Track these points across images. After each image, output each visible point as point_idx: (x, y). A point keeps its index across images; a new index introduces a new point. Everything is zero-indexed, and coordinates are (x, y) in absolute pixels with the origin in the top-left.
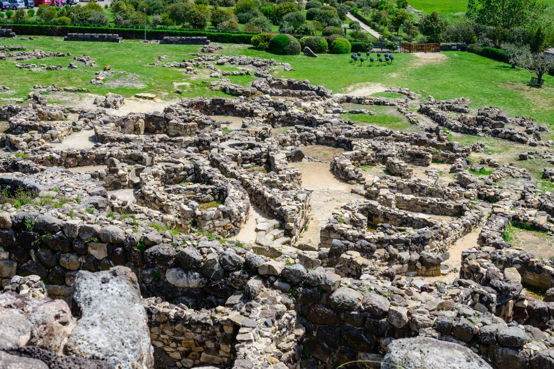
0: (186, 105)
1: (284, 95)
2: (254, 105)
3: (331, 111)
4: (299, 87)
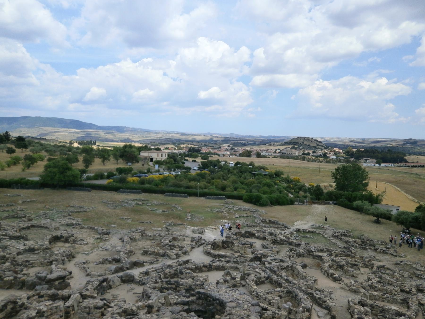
0: (234, 234)
2: (264, 234)
3: (294, 236)
4: (273, 223)
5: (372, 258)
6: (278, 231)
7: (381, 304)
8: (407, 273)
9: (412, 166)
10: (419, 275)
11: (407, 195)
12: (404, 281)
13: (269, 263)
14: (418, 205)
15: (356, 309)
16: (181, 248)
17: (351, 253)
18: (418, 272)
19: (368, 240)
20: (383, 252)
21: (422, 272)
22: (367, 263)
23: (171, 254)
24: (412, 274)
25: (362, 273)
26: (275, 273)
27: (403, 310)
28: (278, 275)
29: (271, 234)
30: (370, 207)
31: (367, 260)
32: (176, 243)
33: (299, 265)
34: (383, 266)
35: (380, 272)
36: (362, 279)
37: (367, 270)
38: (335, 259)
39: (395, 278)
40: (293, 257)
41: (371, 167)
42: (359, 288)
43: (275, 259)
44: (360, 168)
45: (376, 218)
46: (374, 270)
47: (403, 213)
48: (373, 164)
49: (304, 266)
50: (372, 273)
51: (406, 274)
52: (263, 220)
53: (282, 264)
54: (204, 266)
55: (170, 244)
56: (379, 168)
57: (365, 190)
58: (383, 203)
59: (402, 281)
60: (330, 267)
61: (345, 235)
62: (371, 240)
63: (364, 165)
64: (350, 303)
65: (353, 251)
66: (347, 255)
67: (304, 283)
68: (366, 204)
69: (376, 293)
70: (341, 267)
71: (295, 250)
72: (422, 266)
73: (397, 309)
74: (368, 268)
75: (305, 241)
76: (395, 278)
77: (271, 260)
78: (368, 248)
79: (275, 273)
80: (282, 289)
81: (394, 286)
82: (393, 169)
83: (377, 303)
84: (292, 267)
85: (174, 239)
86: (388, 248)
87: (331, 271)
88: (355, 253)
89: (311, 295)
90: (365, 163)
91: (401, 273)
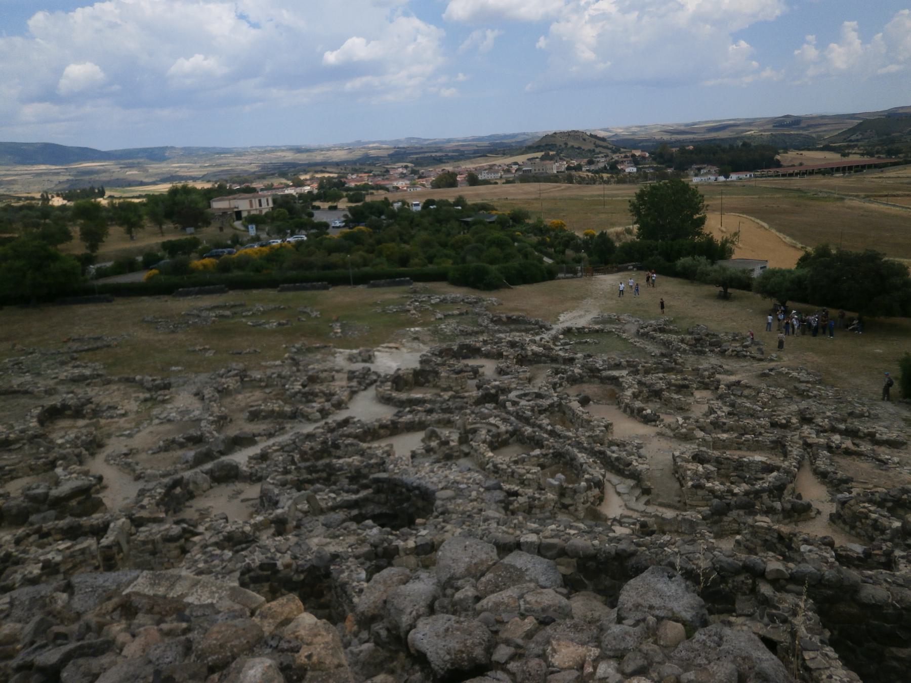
5: (715, 370)
7: (735, 455)
8: (782, 390)
9: (791, 175)
10: (804, 391)
11: (781, 236)
12: (777, 405)
13: (515, 403)
14: (801, 254)
15: (689, 470)
16: (329, 396)
17: (676, 364)
18: (803, 386)
19: (707, 335)
20: (738, 356)
21: (810, 385)
22: (707, 380)
23: (309, 410)
24: (791, 391)
25: (698, 402)
26: (527, 421)
27: (777, 461)
28: (533, 425)
29: (513, 344)
30: (709, 268)
31: (706, 373)
32: (317, 388)
33: (574, 400)
34: (739, 382)
35: (733, 394)
36: (698, 412)
37: (707, 394)
39: (760, 403)
40: (561, 385)
41: (710, 184)
42: (693, 429)
43: (525, 395)
44: (686, 188)
45: (721, 289)
46: (720, 392)
47: (774, 273)
48: (713, 178)
50: (717, 399)
51: (780, 393)
52: (495, 319)
53: (540, 402)
54: (382, 426)
55: (303, 390)
56: (725, 184)
57: (699, 234)
58: (734, 257)
59: (773, 407)
60: (635, 396)
61: (662, 330)
62: (714, 335)
63: (696, 180)
64: (678, 460)
65: (680, 360)
66: (667, 370)
67: (587, 434)
68: (702, 263)
69: (725, 436)
70: (656, 394)
72: (809, 374)
73: (764, 459)
74: (708, 389)
75: (581, 351)
76: (760, 403)
77: (517, 396)
78: (707, 350)
79: (527, 421)
80: (544, 451)
81: (759, 418)
82: (753, 184)
83: (728, 454)
84: (560, 405)
85: (313, 379)
86: (747, 346)
87: (638, 404)
88: (683, 364)
89: (601, 456)
90: (696, 175)
91: (771, 392)
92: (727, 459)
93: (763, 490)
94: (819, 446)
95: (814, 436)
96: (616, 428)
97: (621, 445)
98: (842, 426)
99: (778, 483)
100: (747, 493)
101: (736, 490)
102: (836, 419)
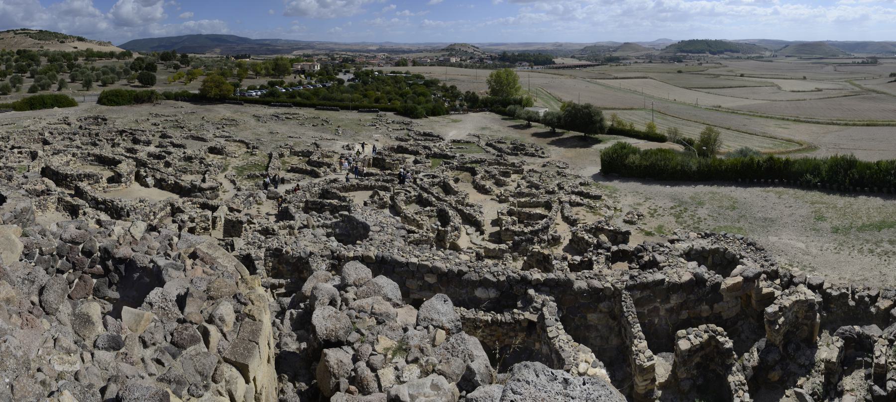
1: (425, 140)
5: (523, 163)
6: (431, 144)
7: (527, 210)
13: (422, 180)
20: (533, 155)
26: (425, 190)
28: (429, 193)
29: (425, 147)
38: (487, 169)
40: (446, 171)
42: (508, 197)
49: (457, 181)
60: (482, 178)
61: (499, 142)
64: (500, 214)
66: (499, 164)
67: (455, 199)
69: (523, 200)
71: (449, 163)
75: (460, 152)
79: (425, 190)
80: (432, 208)
81: (540, 189)
86: (538, 151)
87: (483, 183)
89: (460, 212)
92: (524, 212)
93: (539, 230)
94: (566, 202)
95: (564, 197)
96: (471, 196)
97: (472, 206)
98: (576, 190)
99: (546, 225)
100: (531, 232)
101: (526, 231)
102: (574, 187)
